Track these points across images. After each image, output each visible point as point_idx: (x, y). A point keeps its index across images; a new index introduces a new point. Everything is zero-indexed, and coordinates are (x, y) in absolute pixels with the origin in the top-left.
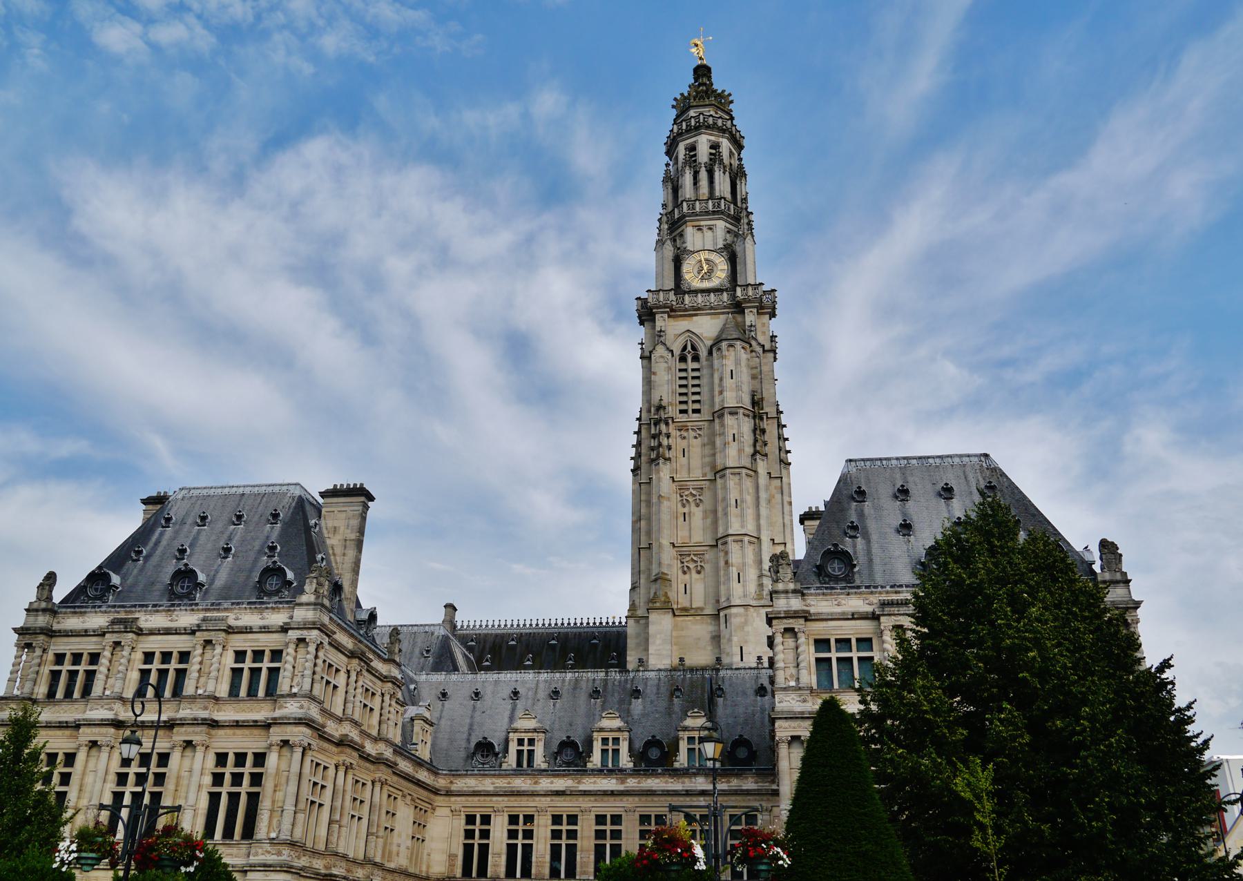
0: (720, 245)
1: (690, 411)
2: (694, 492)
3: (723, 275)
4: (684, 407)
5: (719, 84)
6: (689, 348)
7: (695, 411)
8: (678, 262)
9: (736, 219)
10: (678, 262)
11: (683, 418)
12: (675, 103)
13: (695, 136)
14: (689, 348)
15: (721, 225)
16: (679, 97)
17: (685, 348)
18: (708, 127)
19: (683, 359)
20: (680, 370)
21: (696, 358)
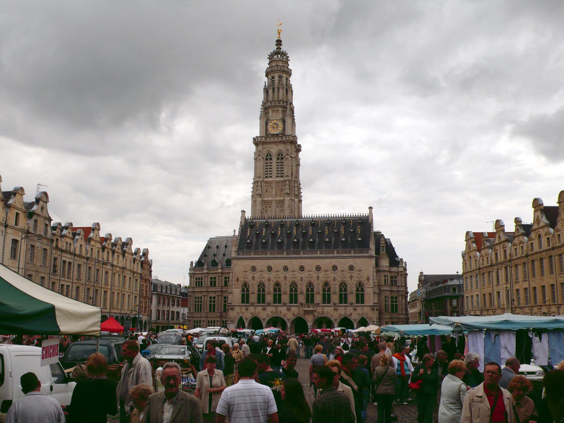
0: (280, 118)
1: (269, 177)
2: (269, 204)
3: (281, 129)
4: (266, 176)
5: (283, 48)
6: (269, 156)
7: (270, 177)
8: (267, 124)
9: (285, 107)
10: (267, 124)
11: (266, 180)
12: (268, 57)
13: (274, 73)
14: (269, 156)
15: (280, 109)
16: (270, 54)
17: (267, 156)
18: (278, 71)
19: (267, 159)
20: (266, 163)
21: (271, 159)
